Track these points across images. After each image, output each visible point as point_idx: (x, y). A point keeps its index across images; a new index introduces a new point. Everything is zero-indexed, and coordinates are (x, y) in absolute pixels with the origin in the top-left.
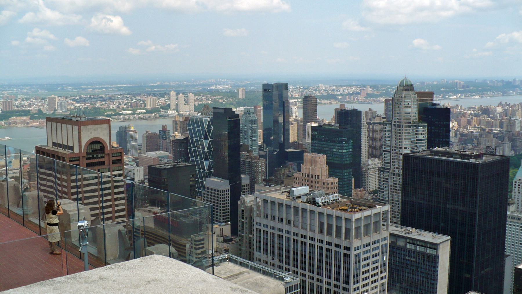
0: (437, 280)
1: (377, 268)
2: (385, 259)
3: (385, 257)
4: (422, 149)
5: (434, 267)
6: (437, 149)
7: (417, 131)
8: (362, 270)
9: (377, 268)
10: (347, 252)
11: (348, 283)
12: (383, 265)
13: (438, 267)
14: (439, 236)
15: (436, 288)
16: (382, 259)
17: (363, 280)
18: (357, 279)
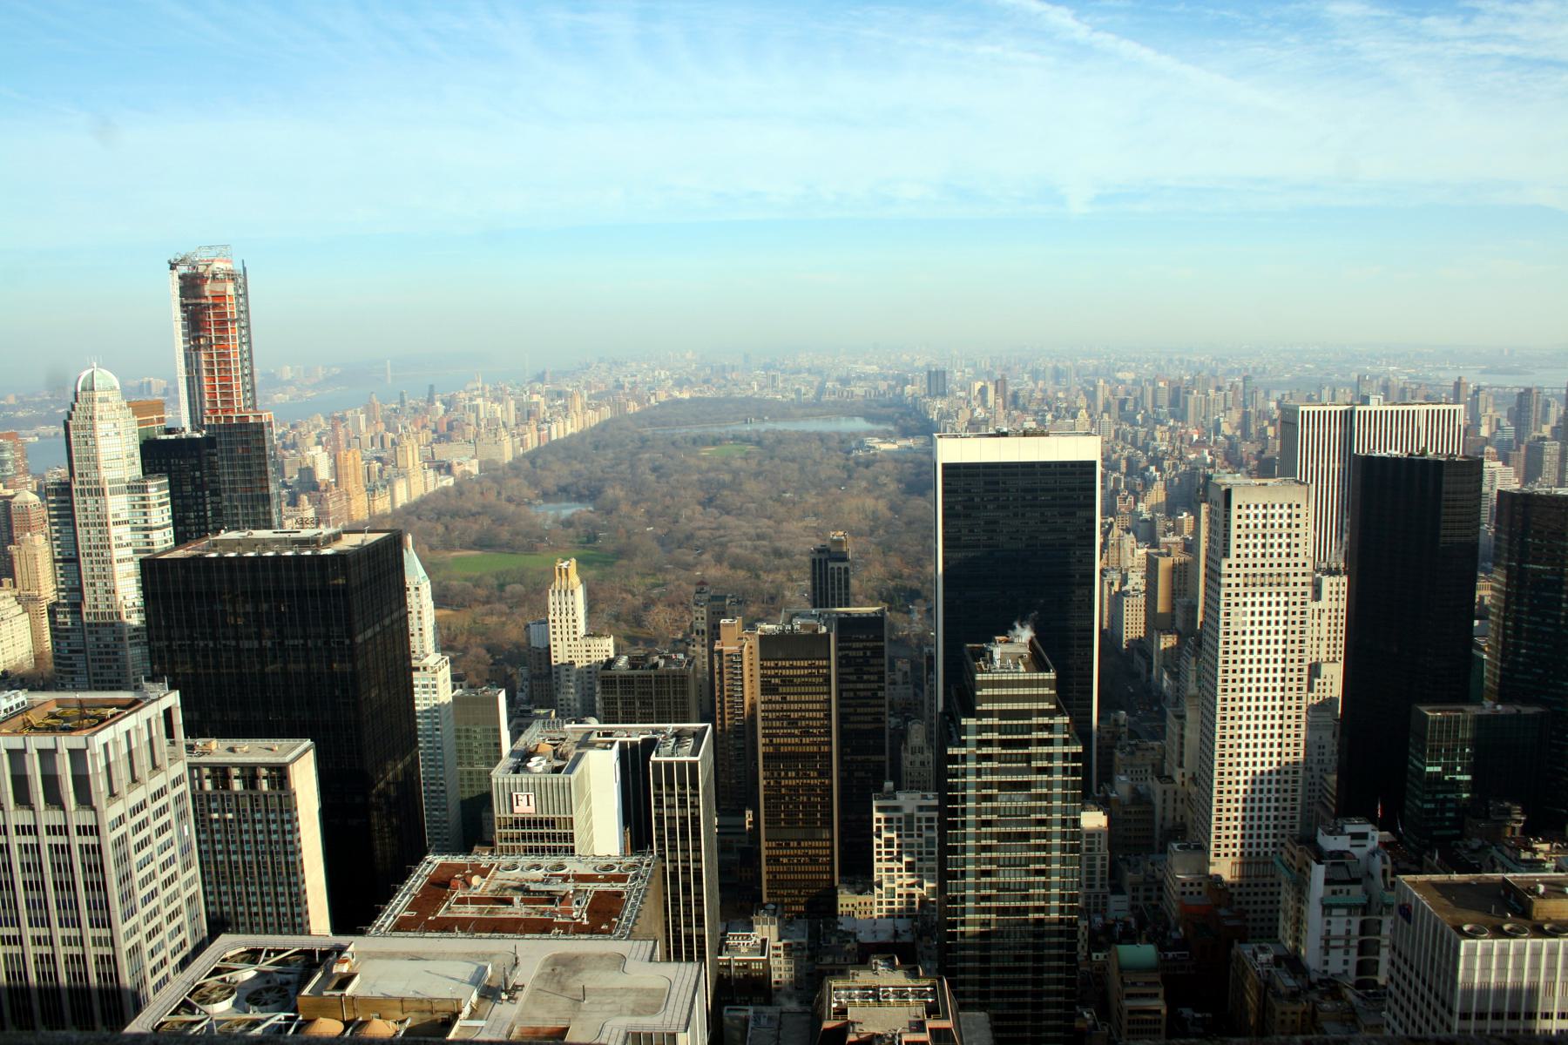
0: (300, 850)
1: (171, 860)
2: (186, 833)
3: (186, 827)
4: (163, 539)
5: (289, 822)
6: (224, 535)
7: (143, 499)
8: (138, 876)
9: (171, 860)
10: (91, 840)
11: (107, 923)
12: (185, 850)
13: (297, 819)
14: (286, 743)
15: (303, 871)
16: (181, 832)
17: (146, 901)
18: (128, 905)
